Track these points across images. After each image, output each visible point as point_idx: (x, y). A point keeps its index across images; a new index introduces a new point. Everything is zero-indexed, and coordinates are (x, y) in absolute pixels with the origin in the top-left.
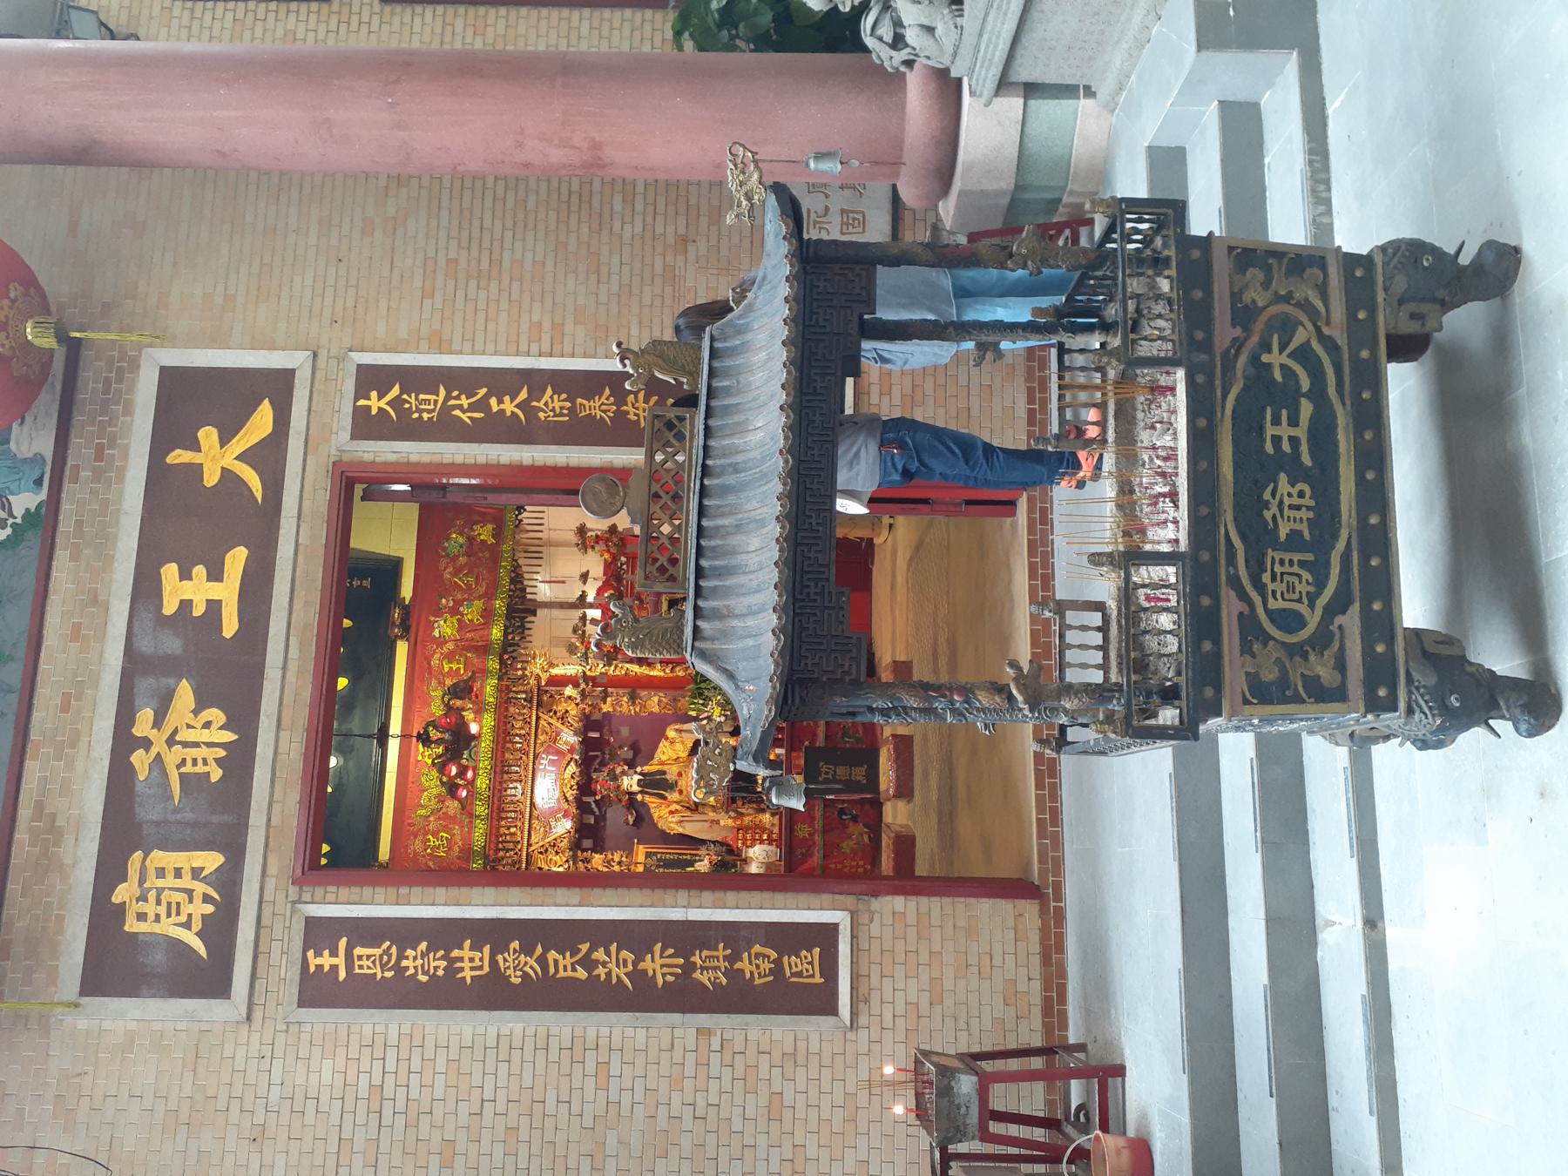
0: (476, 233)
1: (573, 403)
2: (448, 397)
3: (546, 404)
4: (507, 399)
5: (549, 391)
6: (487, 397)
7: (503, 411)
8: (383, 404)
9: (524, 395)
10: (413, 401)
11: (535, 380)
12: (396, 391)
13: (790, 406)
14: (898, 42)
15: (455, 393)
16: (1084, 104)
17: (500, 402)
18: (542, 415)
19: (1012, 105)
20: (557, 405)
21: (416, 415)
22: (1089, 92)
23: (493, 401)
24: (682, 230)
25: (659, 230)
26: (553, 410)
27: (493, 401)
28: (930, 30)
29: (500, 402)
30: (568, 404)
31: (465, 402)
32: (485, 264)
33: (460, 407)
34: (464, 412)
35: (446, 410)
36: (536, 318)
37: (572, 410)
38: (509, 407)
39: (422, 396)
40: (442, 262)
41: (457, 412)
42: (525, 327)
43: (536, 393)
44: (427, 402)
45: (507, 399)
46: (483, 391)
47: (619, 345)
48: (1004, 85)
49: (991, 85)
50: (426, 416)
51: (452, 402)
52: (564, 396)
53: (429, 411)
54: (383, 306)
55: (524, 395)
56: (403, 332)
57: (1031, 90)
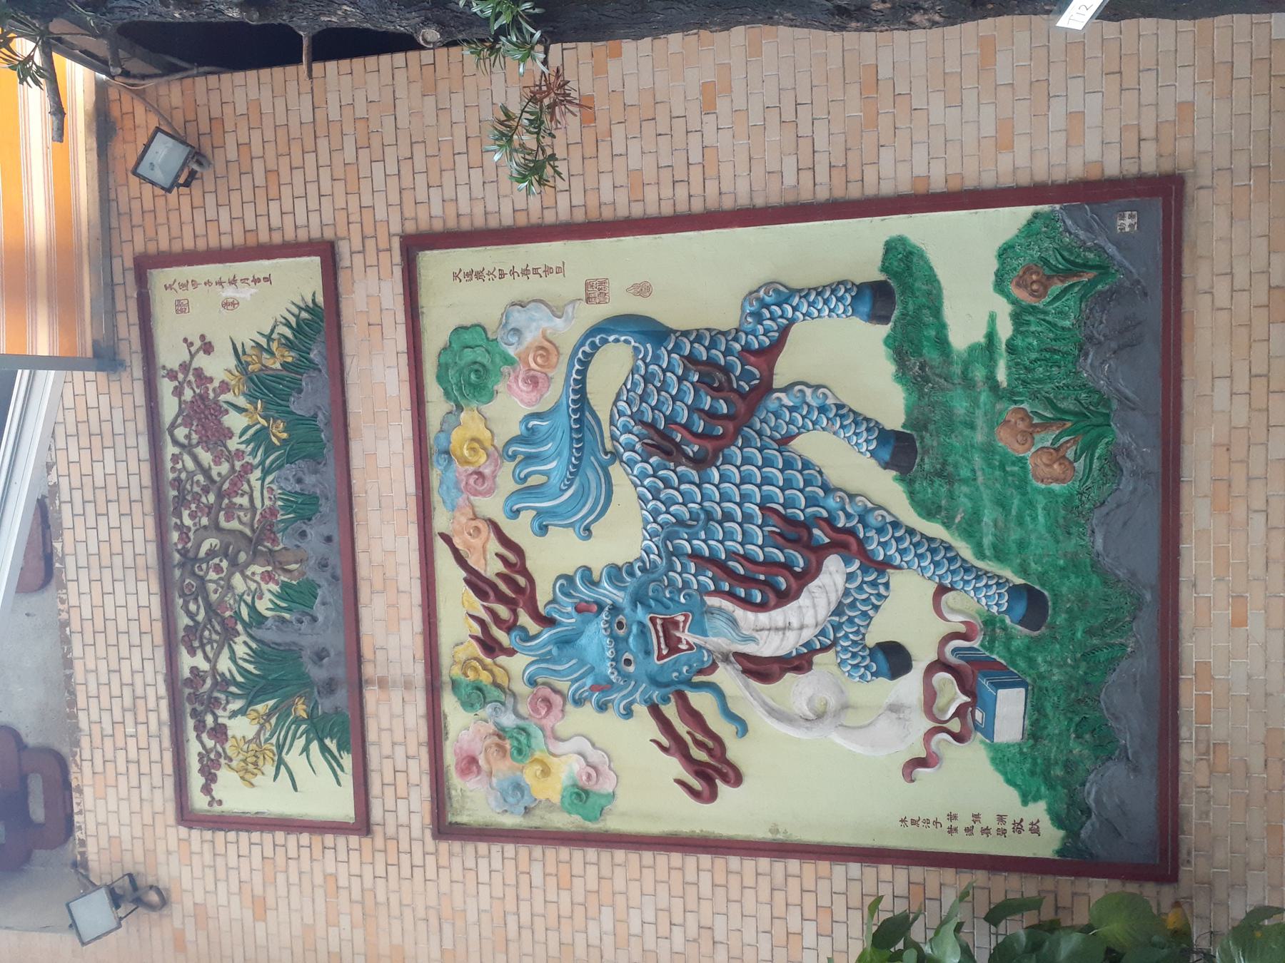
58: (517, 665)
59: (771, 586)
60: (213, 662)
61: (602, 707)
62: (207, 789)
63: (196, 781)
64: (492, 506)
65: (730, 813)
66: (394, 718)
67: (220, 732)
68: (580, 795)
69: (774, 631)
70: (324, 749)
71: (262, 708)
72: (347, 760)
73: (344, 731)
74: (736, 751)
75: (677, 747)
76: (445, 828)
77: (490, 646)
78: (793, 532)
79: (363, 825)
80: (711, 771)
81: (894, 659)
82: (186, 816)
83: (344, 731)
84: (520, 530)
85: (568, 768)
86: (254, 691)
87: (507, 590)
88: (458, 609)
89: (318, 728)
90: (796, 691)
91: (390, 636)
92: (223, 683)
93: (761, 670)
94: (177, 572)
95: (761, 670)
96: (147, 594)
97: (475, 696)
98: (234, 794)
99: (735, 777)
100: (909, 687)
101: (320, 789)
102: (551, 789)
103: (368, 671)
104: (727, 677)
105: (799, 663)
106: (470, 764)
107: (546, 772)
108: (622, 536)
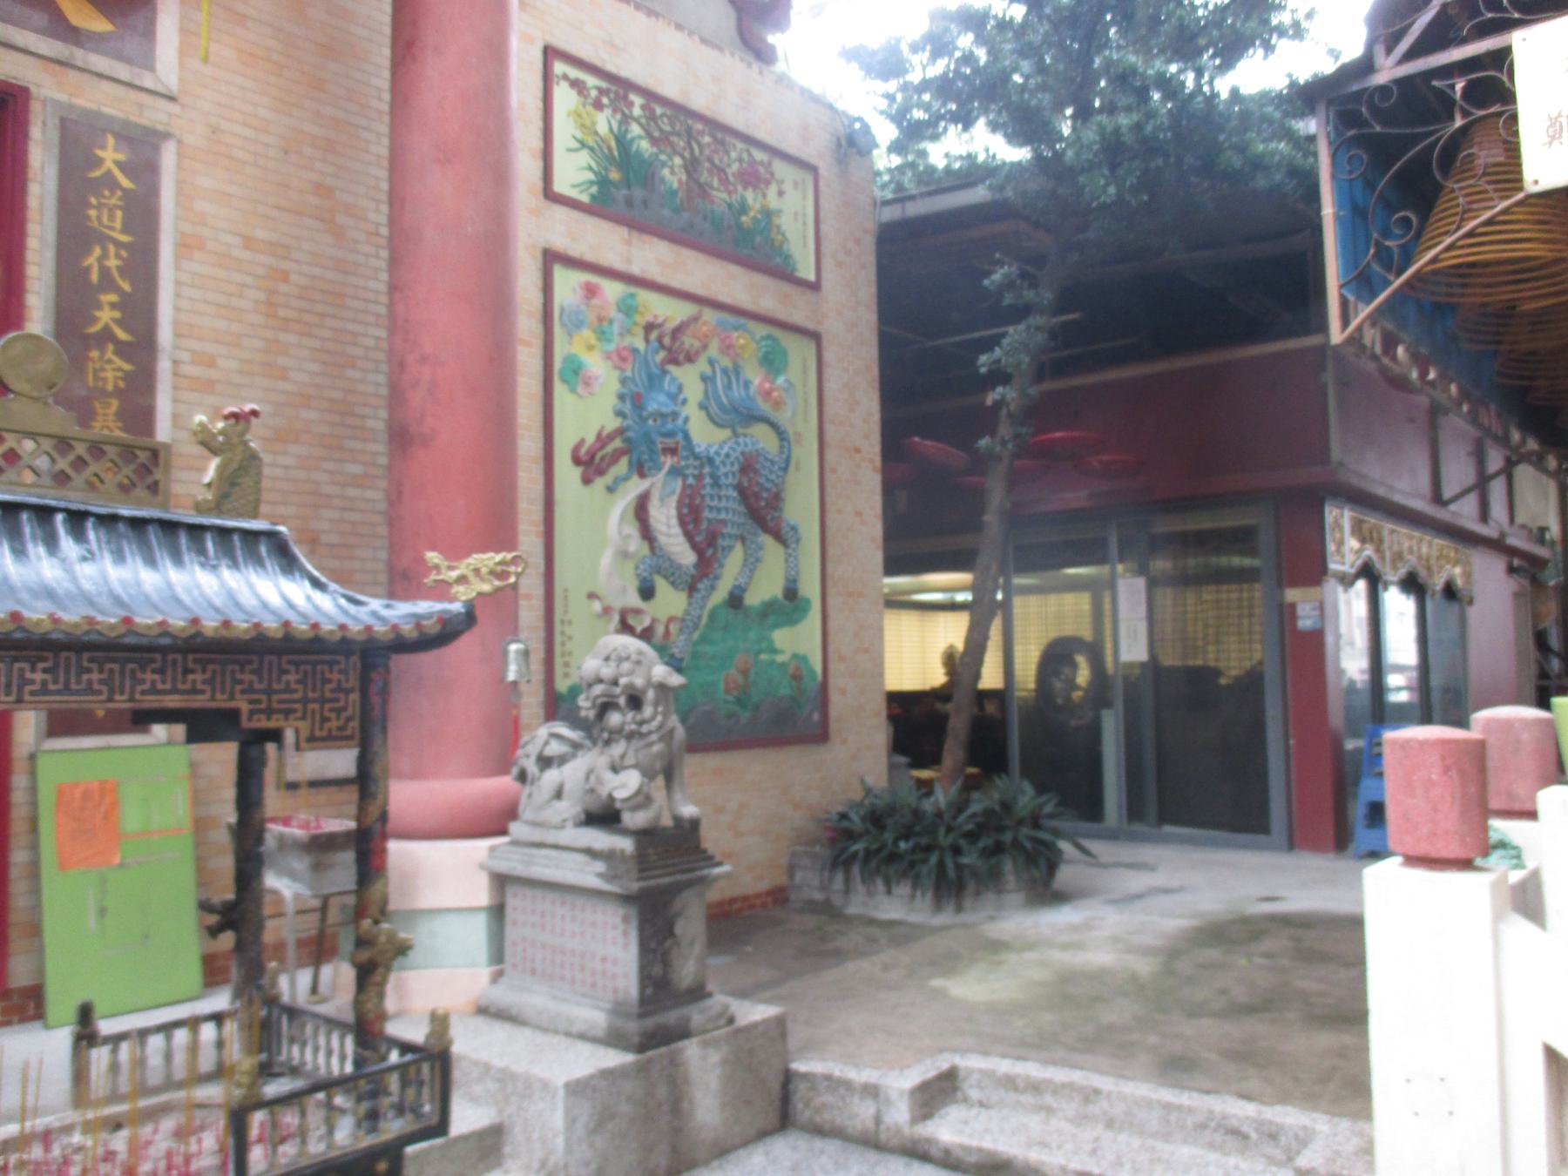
0: (320, 308)
1: (110, 395)
2: (116, 243)
3: (110, 361)
4: (117, 314)
5: (127, 367)
6: (118, 290)
7: (99, 307)
8: (109, 164)
9: (122, 335)
10: (114, 201)
11: (142, 349)
12: (126, 183)
13: (198, 634)
14: (545, 762)
15: (124, 254)
16: (485, 973)
17: (113, 306)
18: (95, 354)
19: (481, 895)
20: (109, 375)
21: (93, 201)
22: (497, 977)
23: (112, 298)
24: (325, 538)
25: (325, 513)
26: (103, 370)
27: (112, 298)
28: (558, 795)
29: (113, 306)
30: (110, 387)
31: (113, 263)
32: (282, 313)
33: (105, 255)
34: (99, 260)
35: (103, 240)
36: (221, 362)
37: (103, 393)
38: (106, 316)
39: (119, 214)
40: (285, 265)
41: (97, 252)
42: (210, 348)
43: (123, 350)
44: (112, 217)
45: (117, 314)
46: (126, 287)
47: (254, 413)
48: (501, 882)
49: (504, 866)
50: (93, 213)
51: (112, 249)
52: (122, 384)
53: (99, 218)
54: (232, 189)
55: (122, 335)
56: (201, 206)
57: (498, 912)
58: (640, 344)
60: (637, 120)
61: (621, 397)
62: (565, 77)
63: (574, 73)
64: (713, 350)
65: (567, 474)
67: (598, 105)
68: (576, 371)
69: (664, 517)
70: (592, 183)
71: (613, 144)
72: (585, 198)
73: (603, 205)
74: (600, 483)
75: (603, 440)
77: (649, 327)
78: (712, 538)
80: (591, 464)
81: (647, 592)
84: (702, 365)
85: (596, 365)
86: (622, 141)
87: (673, 347)
88: (669, 311)
89: (603, 182)
90: (632, 529)
92: (626, 119)
93: (641, 509)
95: (641, 509)
96: (670, 90)
97: (627, 308)
98: (564, 97)
99: (587, 480)
100: (634, 600)
101: (573, 172)
102: (578, 349)
103: (635, 234)
104: (636, 487)
105: (647, 533)
106: (591, 291)
107: (590, 348)
108: (704, 435)
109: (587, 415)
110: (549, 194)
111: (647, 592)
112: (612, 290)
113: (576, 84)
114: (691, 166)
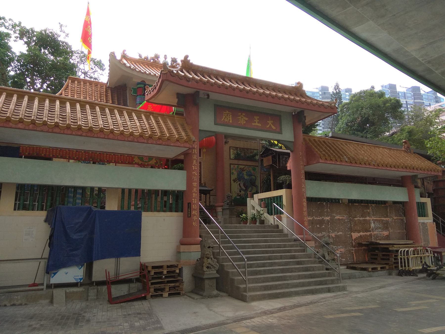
48: (223, 209)
59: (244, 185)
65: (232, 182)
66: (236, 162)
68: (233, 173)
69: (242, 185)
73: (236, 158)
76: (230, 164)
79: (230, 159)
80: (234, 181)
81: (240, 192)
82: (230, 147)
83: (236, 158)
84: (246, 171)
85: (235, 172)
86: (237, 153)
87: (243, 170)
88: (242, 167)
89: (235, 157)
90: (239, 186)
91: (241, 162)
94: (243, 149)
96: (242, 147)
97: (238, 167)
98: (231, 150)
101: (232, 156)
102: (233, 171)
104: (239, 182)
106: (234, 166)
108: (246, 177)
109: (234, 177)
110: (230, 159)
111: (240, 192)
112: (236, 166)
113: (233, 149)
114: (245, 153)
